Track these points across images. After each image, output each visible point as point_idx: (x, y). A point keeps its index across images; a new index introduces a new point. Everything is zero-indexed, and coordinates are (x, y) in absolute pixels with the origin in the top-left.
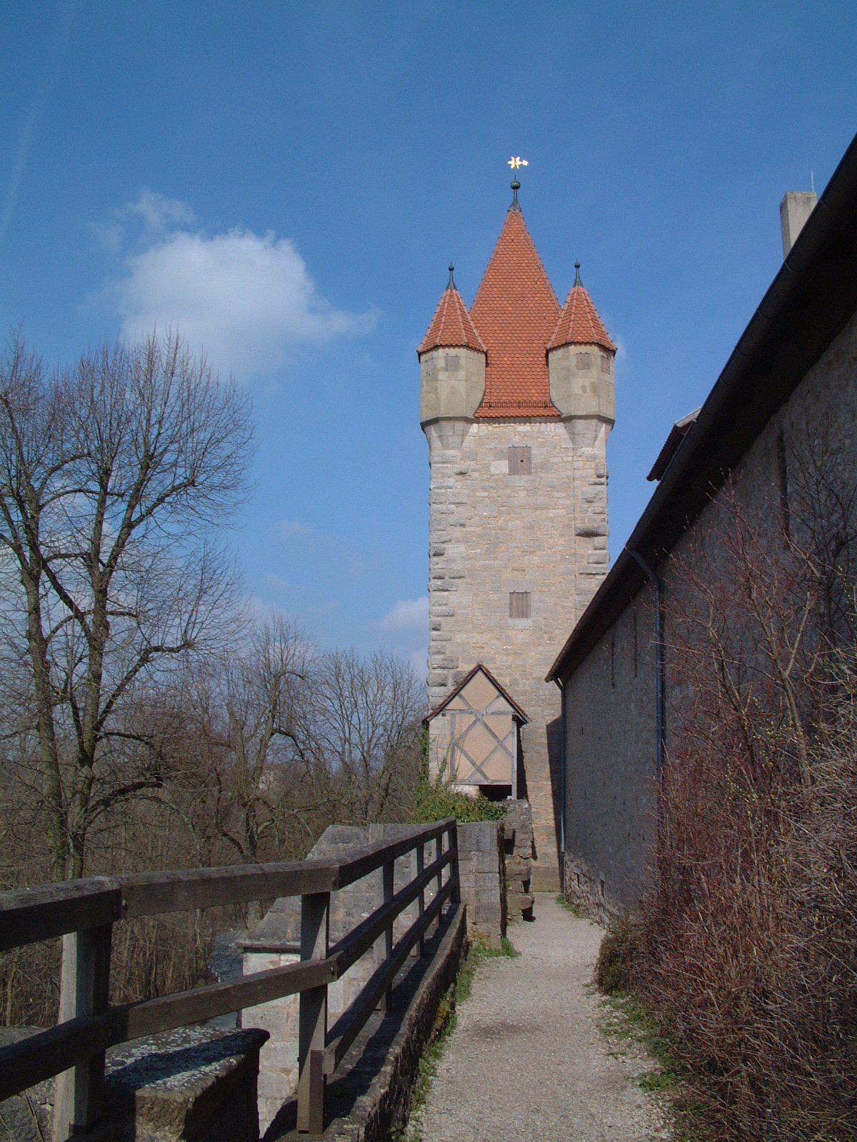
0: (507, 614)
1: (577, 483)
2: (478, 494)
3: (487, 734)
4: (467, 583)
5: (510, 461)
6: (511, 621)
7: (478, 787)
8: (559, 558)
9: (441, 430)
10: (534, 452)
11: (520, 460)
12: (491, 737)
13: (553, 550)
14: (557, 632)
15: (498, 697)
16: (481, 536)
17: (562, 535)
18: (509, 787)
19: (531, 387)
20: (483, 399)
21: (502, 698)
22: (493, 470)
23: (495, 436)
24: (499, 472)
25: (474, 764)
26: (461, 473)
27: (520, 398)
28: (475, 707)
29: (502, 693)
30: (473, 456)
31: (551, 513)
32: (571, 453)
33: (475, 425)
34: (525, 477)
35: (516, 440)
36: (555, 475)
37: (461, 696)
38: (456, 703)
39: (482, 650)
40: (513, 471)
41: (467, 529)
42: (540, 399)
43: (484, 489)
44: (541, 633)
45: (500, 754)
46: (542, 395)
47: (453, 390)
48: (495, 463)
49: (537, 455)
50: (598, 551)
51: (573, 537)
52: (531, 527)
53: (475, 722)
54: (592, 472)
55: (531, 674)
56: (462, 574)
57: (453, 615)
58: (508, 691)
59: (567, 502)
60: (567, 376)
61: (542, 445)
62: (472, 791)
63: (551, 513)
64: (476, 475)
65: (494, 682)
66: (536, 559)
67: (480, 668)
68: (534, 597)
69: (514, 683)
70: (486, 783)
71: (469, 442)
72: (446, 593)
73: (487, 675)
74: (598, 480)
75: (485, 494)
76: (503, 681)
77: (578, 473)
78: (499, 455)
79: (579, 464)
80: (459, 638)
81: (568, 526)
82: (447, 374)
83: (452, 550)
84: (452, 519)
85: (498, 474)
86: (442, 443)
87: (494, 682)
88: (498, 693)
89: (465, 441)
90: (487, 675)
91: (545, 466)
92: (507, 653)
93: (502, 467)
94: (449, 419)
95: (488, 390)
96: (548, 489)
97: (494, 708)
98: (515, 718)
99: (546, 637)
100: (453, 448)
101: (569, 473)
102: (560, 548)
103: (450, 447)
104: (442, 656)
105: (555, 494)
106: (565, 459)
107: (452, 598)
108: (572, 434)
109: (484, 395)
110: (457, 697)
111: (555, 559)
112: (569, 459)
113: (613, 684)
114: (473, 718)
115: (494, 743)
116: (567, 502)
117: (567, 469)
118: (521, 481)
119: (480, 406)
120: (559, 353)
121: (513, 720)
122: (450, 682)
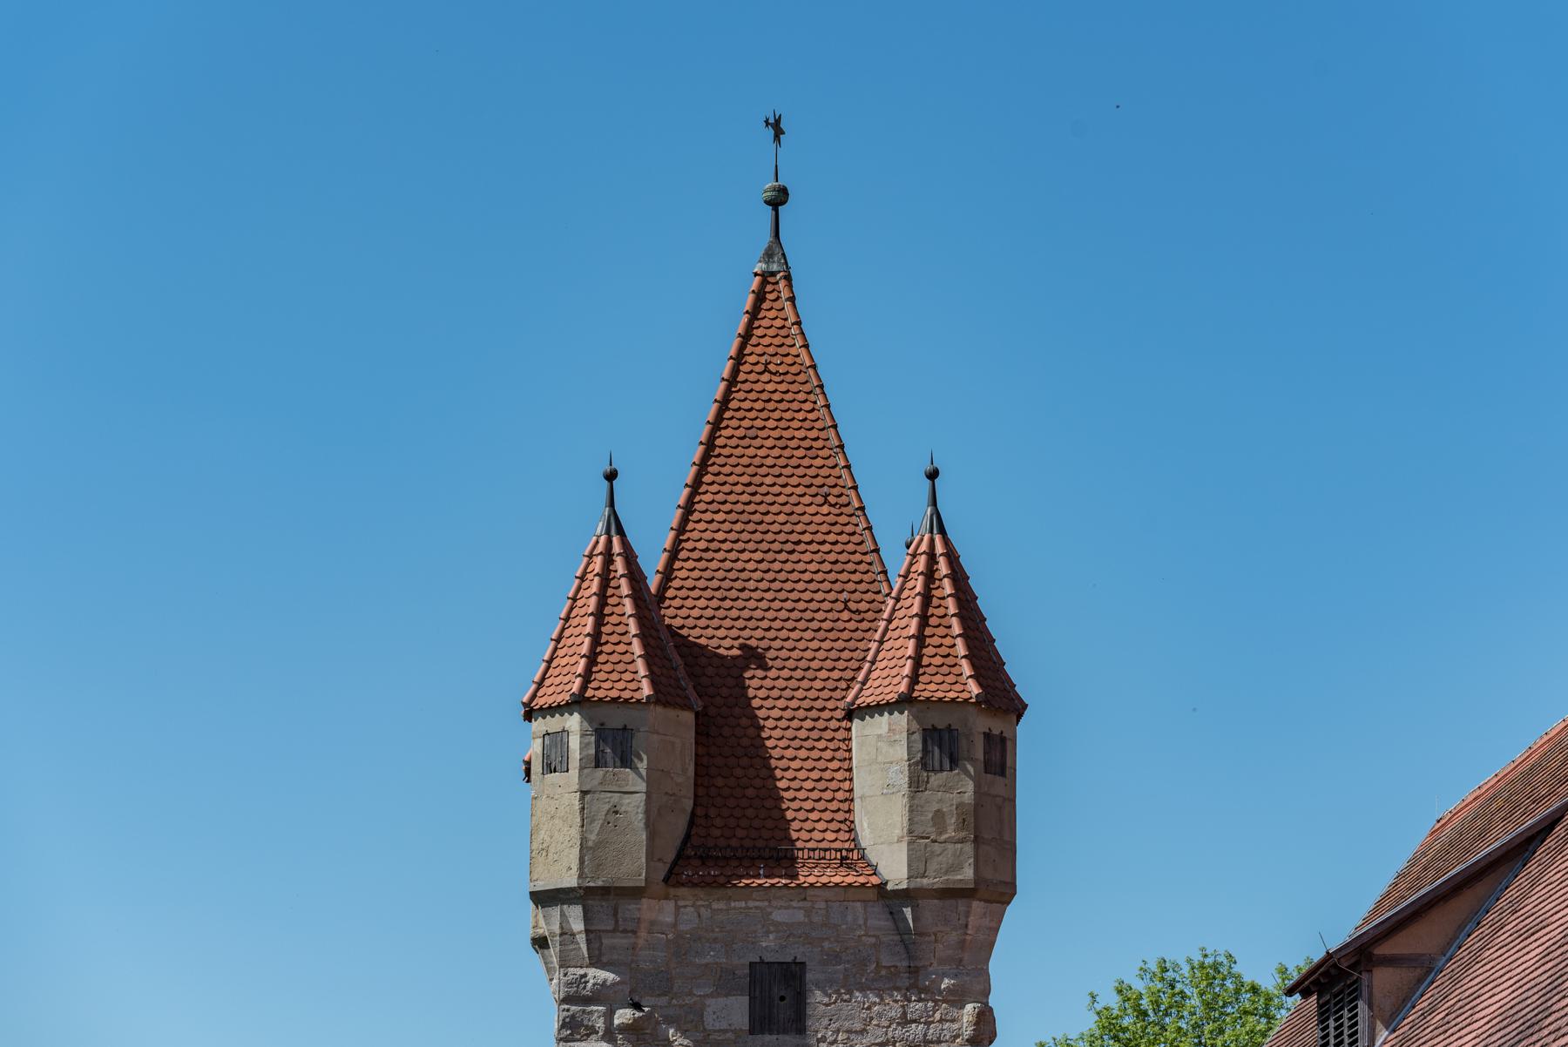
10: (809, 976)
20: (688, 837)
22: (710, 1021)
24: (724, 1026)
33: (669, 906)
35: (770, 947)
40: (761, 1022)
48: (714, 1004)
61: (836, 958)
78: (724, 983)
82: (600, 772)
85: (725, 1031)
93: (734, 1011)
95: (699, 812)
103: (604, 959)
109: (692, 823)
120: (882, 723)
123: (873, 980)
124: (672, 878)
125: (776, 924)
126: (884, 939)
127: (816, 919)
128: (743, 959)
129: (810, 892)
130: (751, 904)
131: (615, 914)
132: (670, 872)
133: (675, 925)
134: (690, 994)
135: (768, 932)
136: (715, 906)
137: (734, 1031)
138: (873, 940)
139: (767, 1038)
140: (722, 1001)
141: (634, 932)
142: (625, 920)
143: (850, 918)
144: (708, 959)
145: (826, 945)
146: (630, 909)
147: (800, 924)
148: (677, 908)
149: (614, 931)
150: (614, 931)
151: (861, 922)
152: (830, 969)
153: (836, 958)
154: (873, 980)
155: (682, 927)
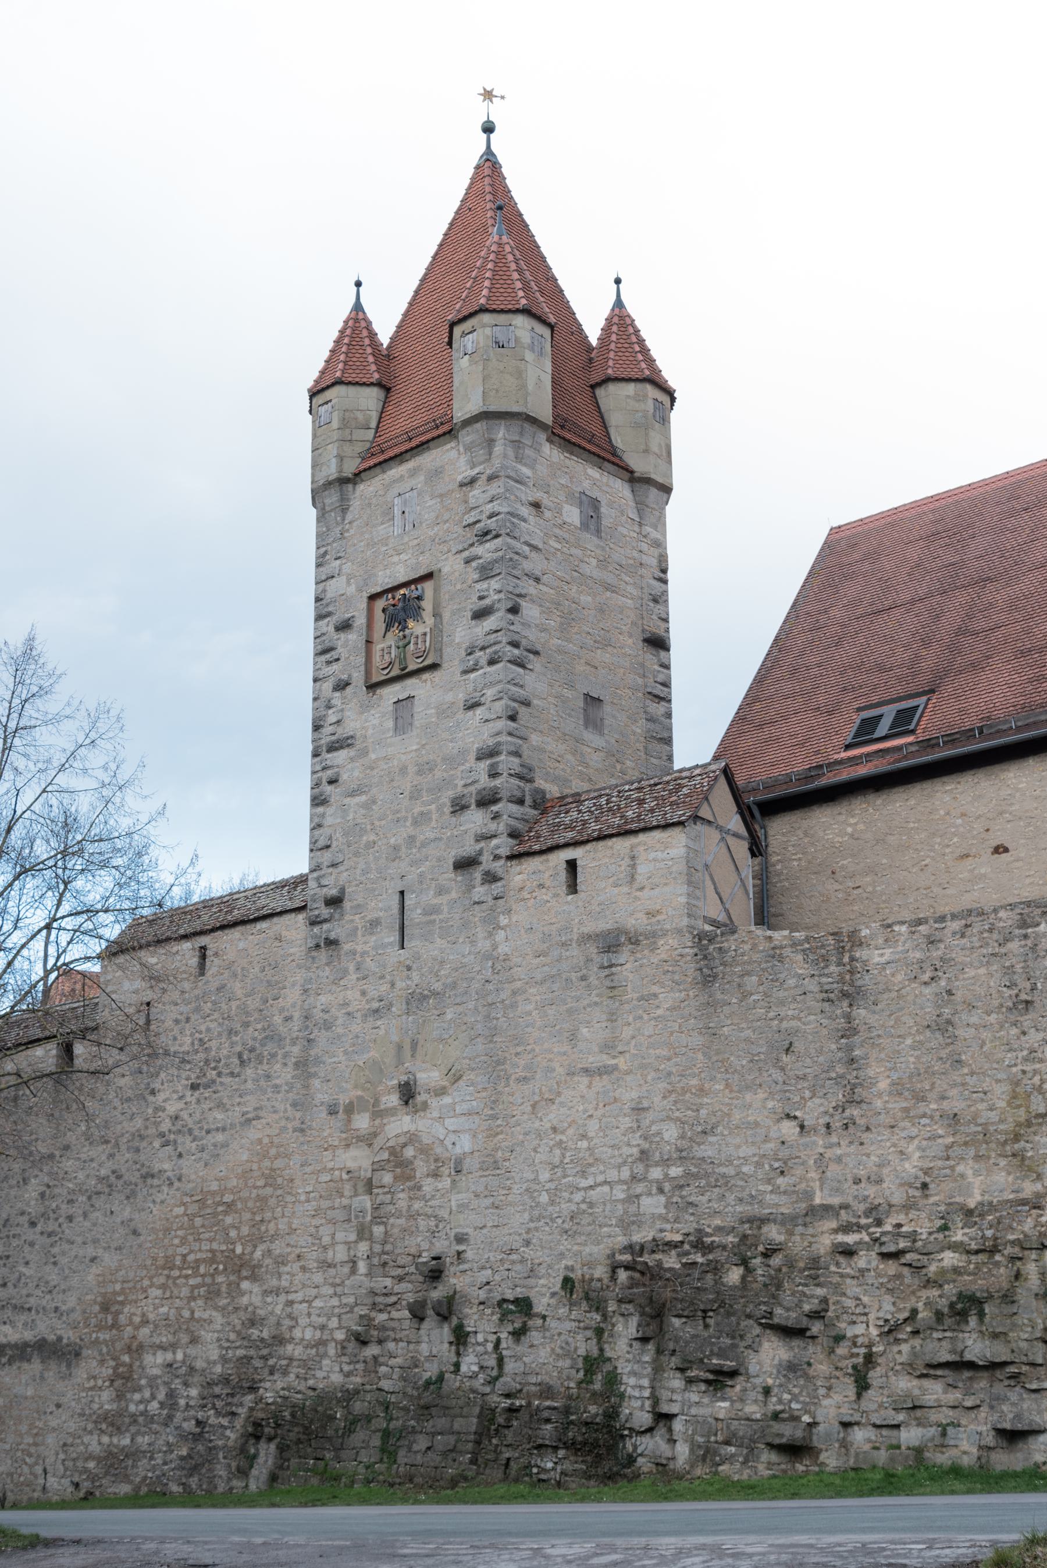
0: (581, 722)
1: (643, 571)
3: (730, 860)
17: (631, 636)
41: (541, 587)
48: (567, 508)
56: (539, 648)
57: (527, 704)
68: (607, 708)
72: (520, 670)
75: (558, 546)
77: (645, 559)
79: (645, 547)
83: (530, 611)
84: (527, 565)
100: (525, 465)
104: (517, 760)
105: (623, 576)
107: (529, 679)
122: (528, 801)
129: (606, 464)
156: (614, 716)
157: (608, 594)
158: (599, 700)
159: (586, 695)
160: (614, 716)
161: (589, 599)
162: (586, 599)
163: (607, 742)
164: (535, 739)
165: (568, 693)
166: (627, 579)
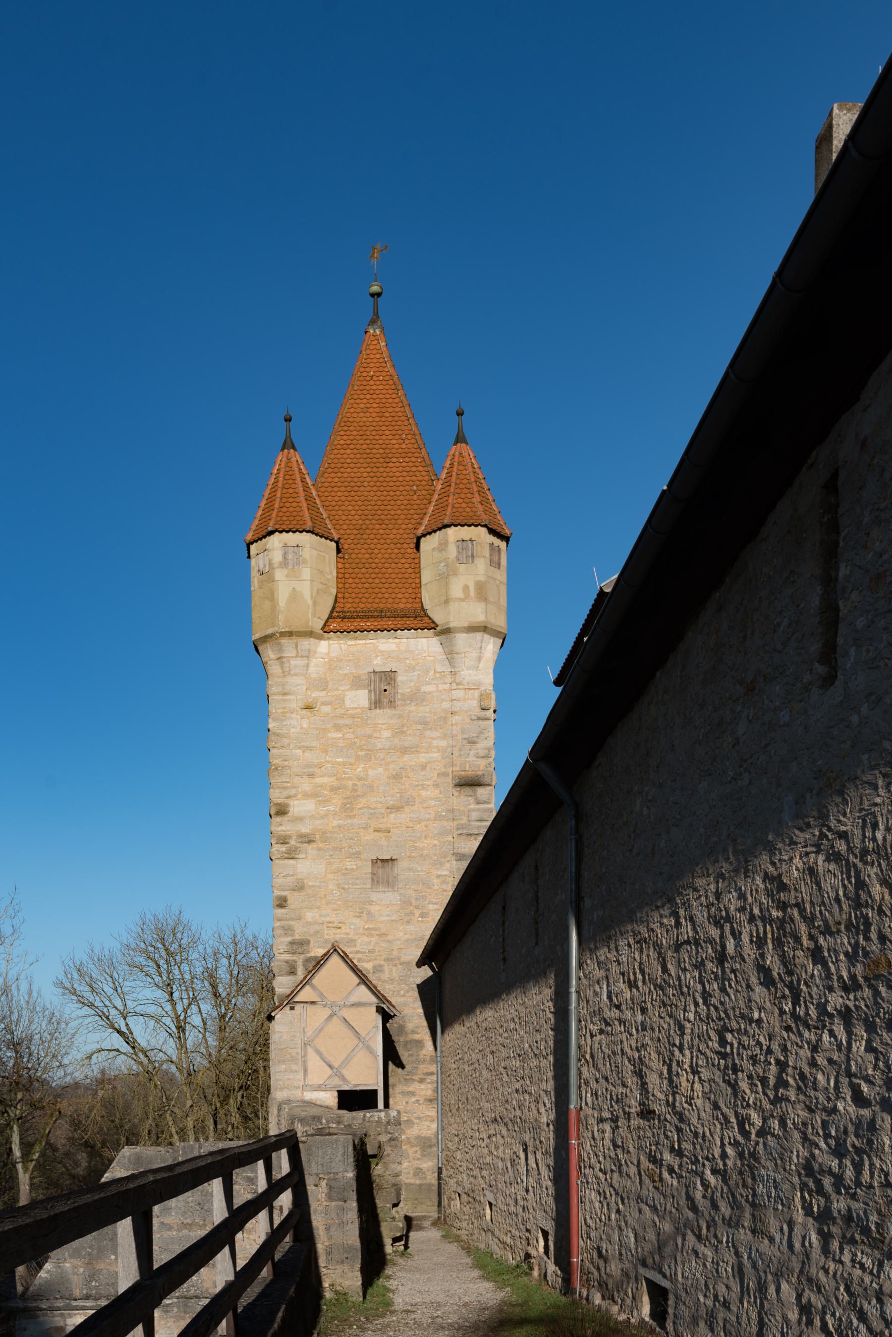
2: (330, 735)
4: (319, 849)
5: (370, 692)
6: (374, 896)
7: (336, 1094)
8: (432, 816)
9: (281, 650)
11: (383, 687)
12: (350, 1034)
13: (425, 805)
14: (431, 907)
15: (358, 984)
16: (334, 789)
17: (436, 785)
18: (375, 1092)
19: (397, 591)
21: (363, 988)
22: (348, 704)
23: (351, 657)
24: (356, 706)
25: (330, 1066)
26: (308, 707)
27: (382, 605)
28: (330, 997)
29: (363, 979)
30: (322, 684)
31: (423, 758)
32: (449, 679)
34: (388, 711)
35: (378, 664)
36: (427, 709)
37: (314, 987)
38: (306, 994)
39: (339, 931)
42: (409, 606)
43: (338, 728)
44: (412, 908)
45: (361, 1056)
46: (410, 600)
47: (295, 595)
48: (350, 694)
49: (405, 683)
50: (481, 806)
51: (451, 789)
52: (397, 777)
53: (331, 1016)
54: (475, 703)
55: (399, 958)
58: (371, 977)
59: (443, 743)
60: (444, 578)
61: (412, 669)
62: (330, 1099)
63: (423, 758)
64: (326, 709)
65: (355, 969)
66: (403, 817)
67: (335, 950)
68: (402, 864)
69: (378, 969)
70: (346, 1088)
71: (316, 667)
73: (345, 958)
74: (484, 713)
76: (366, 966)
77: (457, 706)
78: (356, 683)
80: (309, 916)
81: (445, 774)
86: (282, 668)
87: (355, 969)
88: (357, 980)
89: (312, 664)
90: (345, 958)
91: (417, 697)
92: (369, 932)
93: (360, 698)
94: (290, 634)
96: (419, 727)
97: (353, 999)
98: (380, 1010)
99: (417, 913)
101: (446, 705)
102: (433, 803)
103: (292, 672)
105: (428, 733)
106: (441, 687)
108: (451, 655)
110: (307, 987)
111: (427, 816)
112: (447, 686)
113: (504, 960)
114: (327, 1012)
115: (353, 1042)
116: (443, 743)
117: (443, 700)
118: (383, 716)
119: (330, 617)
121: (377, 1011)
123: (433, 679)
124: (326, 629)
125: (382, 652)
126: (438, 658)
127: (402, 648)
128: (364, 671)
130: (368, 641)
131: (296, 647)
132: (325, 625)
133: (328, 654)
134: (337, 690)
135: (377, 656)
136: (349, 643)
137: (361, 708)
138: (432, 658)
139: (378, 711)
140: (354, 693)
141: (307, 657)
142: (302, 650)
143: (419, 647)
144: (346, 671)
145: (408, 661)
146: (306, 643)
147: (393, 651)
148: (329, 646)
149: (296, 656)
150: (296, 656)
151: (426, 649)
152: (410, 674)
153: (412, 669)
154: (433, 679)
155: (333, 655)
156: (410, 869)
157: (406, 758)
158: (392, 860)
159: (374, 862)
160: (410, 869)
161: (381, 770)
162: (377, 772)
163: (401, 894)
164: (309, 916)
165: (350, 864)
166: (434, 734)
